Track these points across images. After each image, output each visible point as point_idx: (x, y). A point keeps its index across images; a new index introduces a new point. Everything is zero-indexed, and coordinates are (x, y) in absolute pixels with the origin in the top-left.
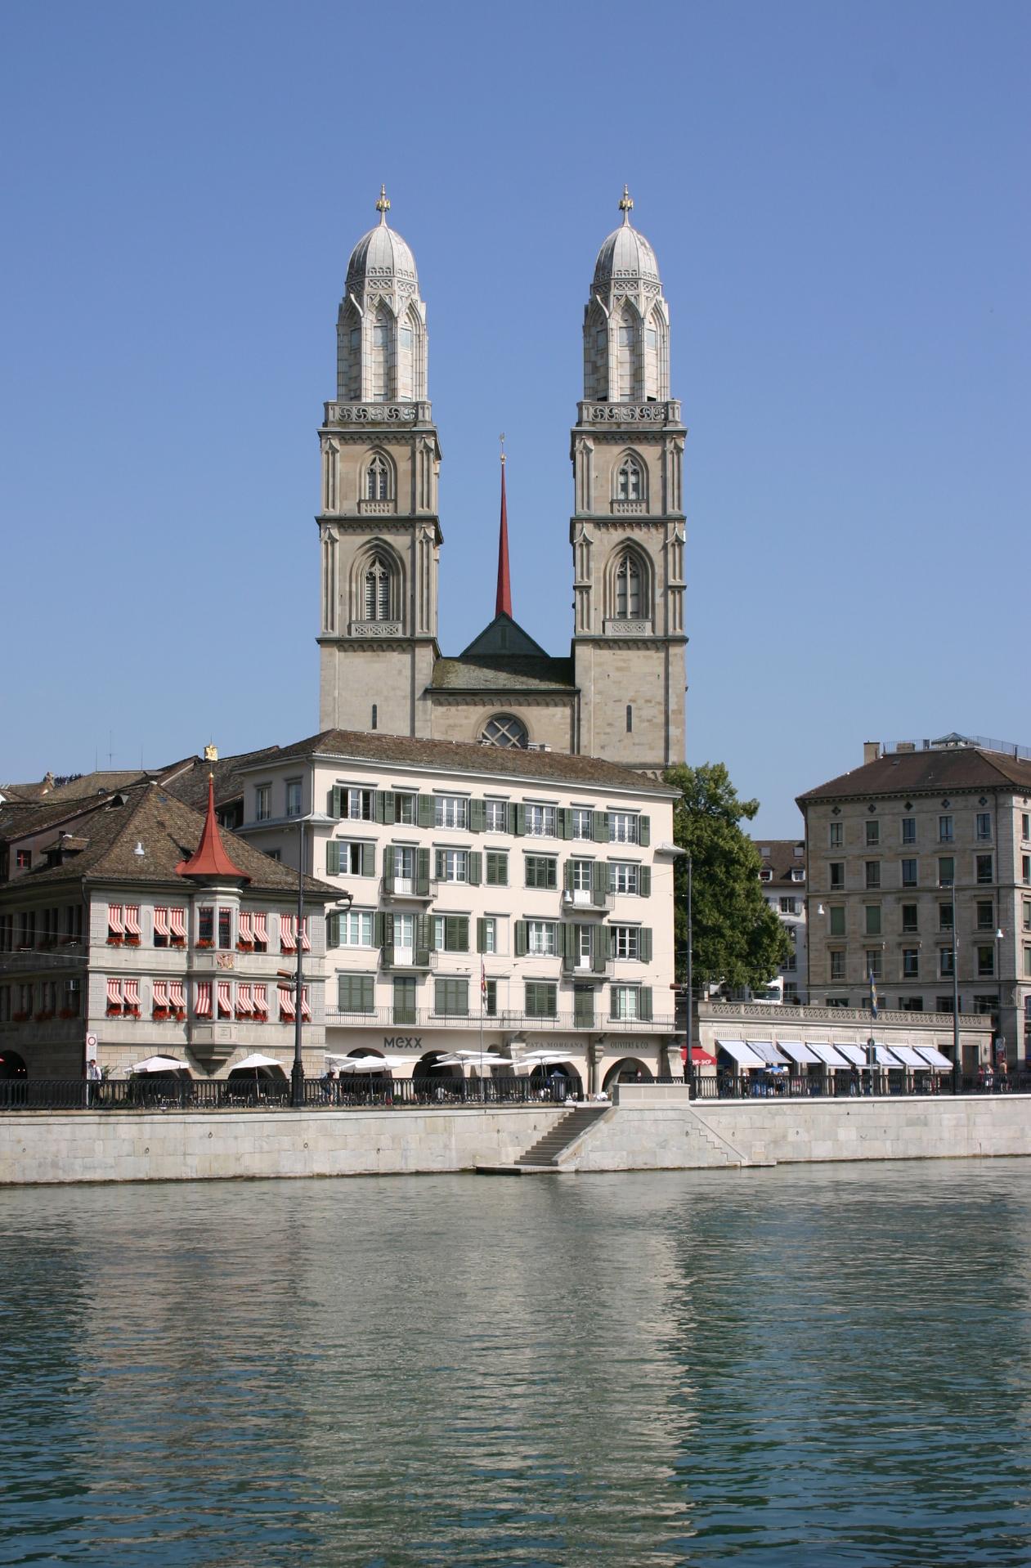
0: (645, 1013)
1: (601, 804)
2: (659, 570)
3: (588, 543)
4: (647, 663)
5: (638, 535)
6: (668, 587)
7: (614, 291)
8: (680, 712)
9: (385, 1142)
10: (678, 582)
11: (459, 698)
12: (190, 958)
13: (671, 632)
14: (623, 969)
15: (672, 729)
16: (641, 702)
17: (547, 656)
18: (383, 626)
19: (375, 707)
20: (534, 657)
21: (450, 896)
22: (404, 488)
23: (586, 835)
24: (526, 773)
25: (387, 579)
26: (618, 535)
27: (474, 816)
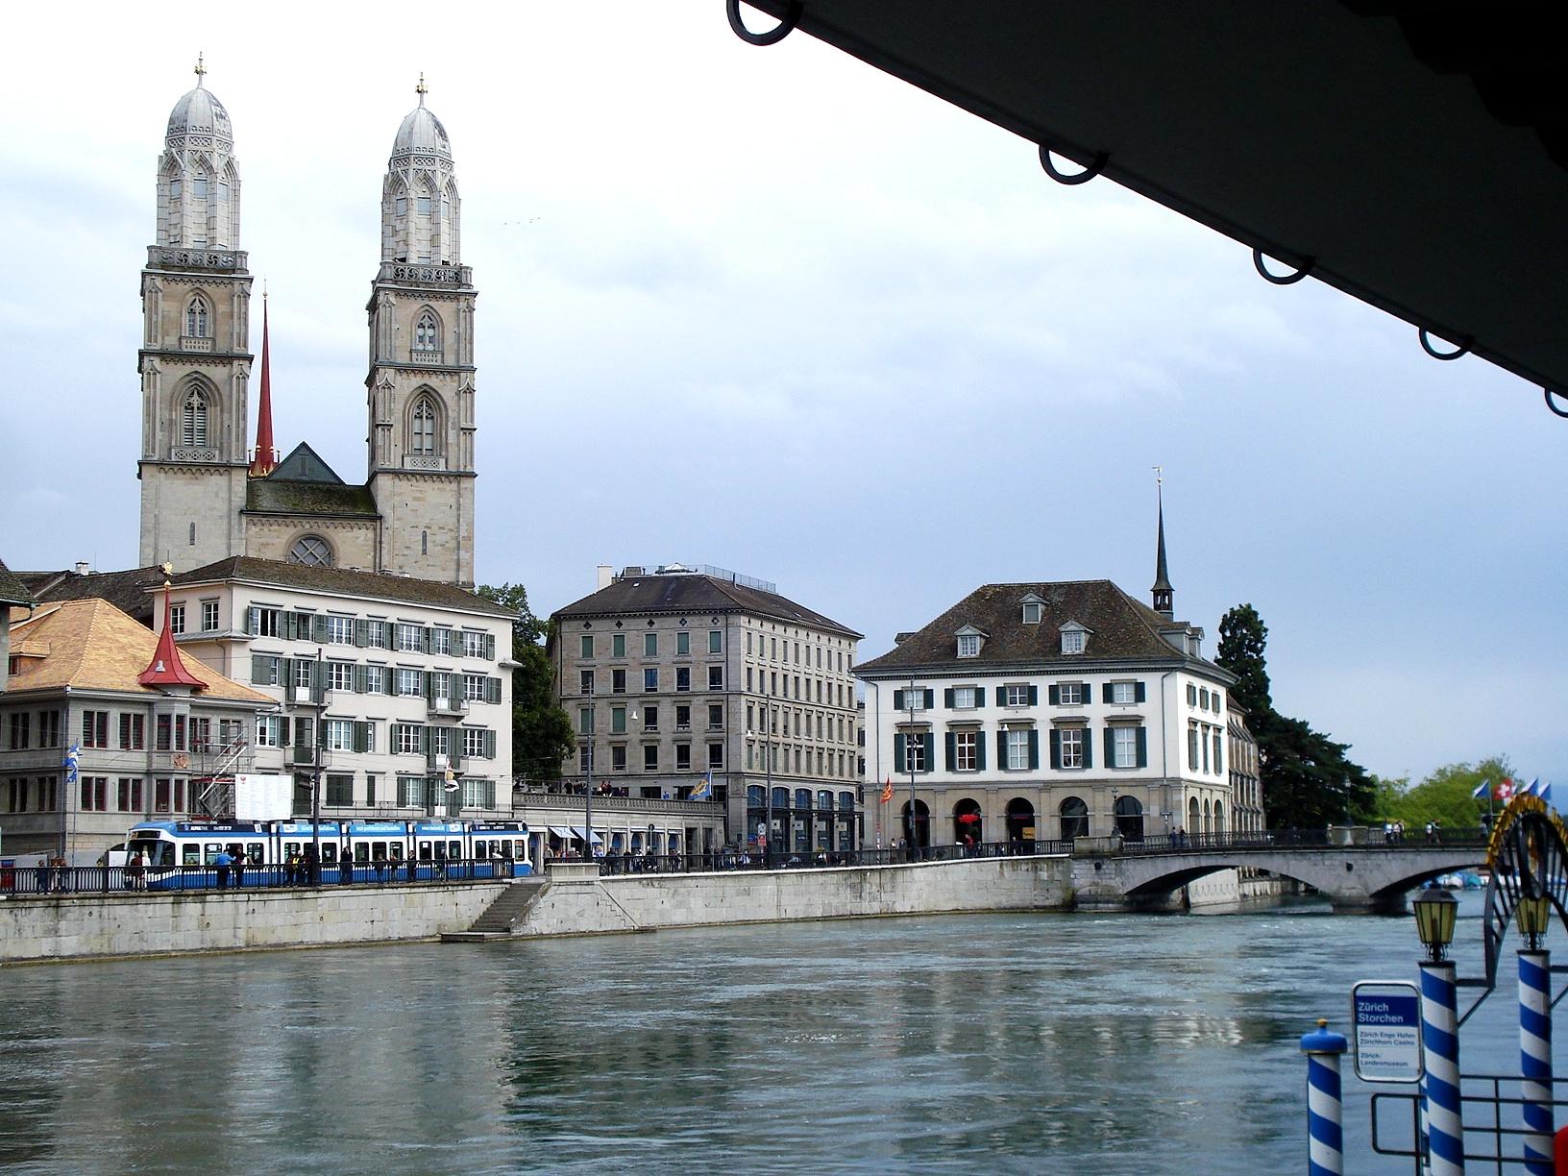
0: (490, 804)
1: (458, 623)
3: (388, 386)
5: (434, 381)
8: (470, 538)
9: (377, 915)
12: (149, 758)
14: (474, 766)
16: (435, 528)
18: (201, 451)
19: (193, 526)
22: (223, 328)
23: (446, 651)
24: (407, 599)
26: (416, 381)
27: (358, 633)
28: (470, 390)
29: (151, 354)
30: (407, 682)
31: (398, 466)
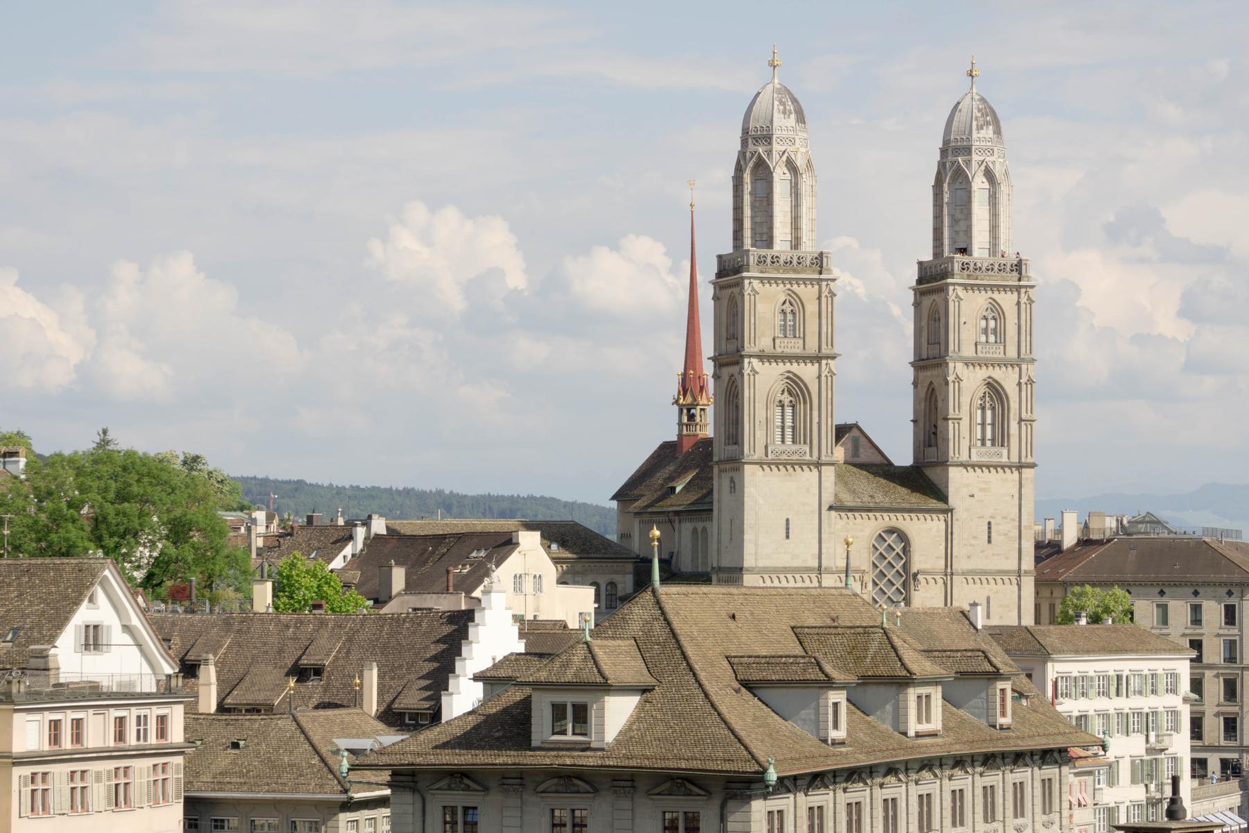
2: (1014, 405)
5: (997, 374)
6: (1021, 420)
7: (976, 157)
13: (1023, 460)
15: (1023, 541)
17: (890, 464)
19: (787, 520)
22: (812, 327)
26: (982, 374)
29: (750, 356)
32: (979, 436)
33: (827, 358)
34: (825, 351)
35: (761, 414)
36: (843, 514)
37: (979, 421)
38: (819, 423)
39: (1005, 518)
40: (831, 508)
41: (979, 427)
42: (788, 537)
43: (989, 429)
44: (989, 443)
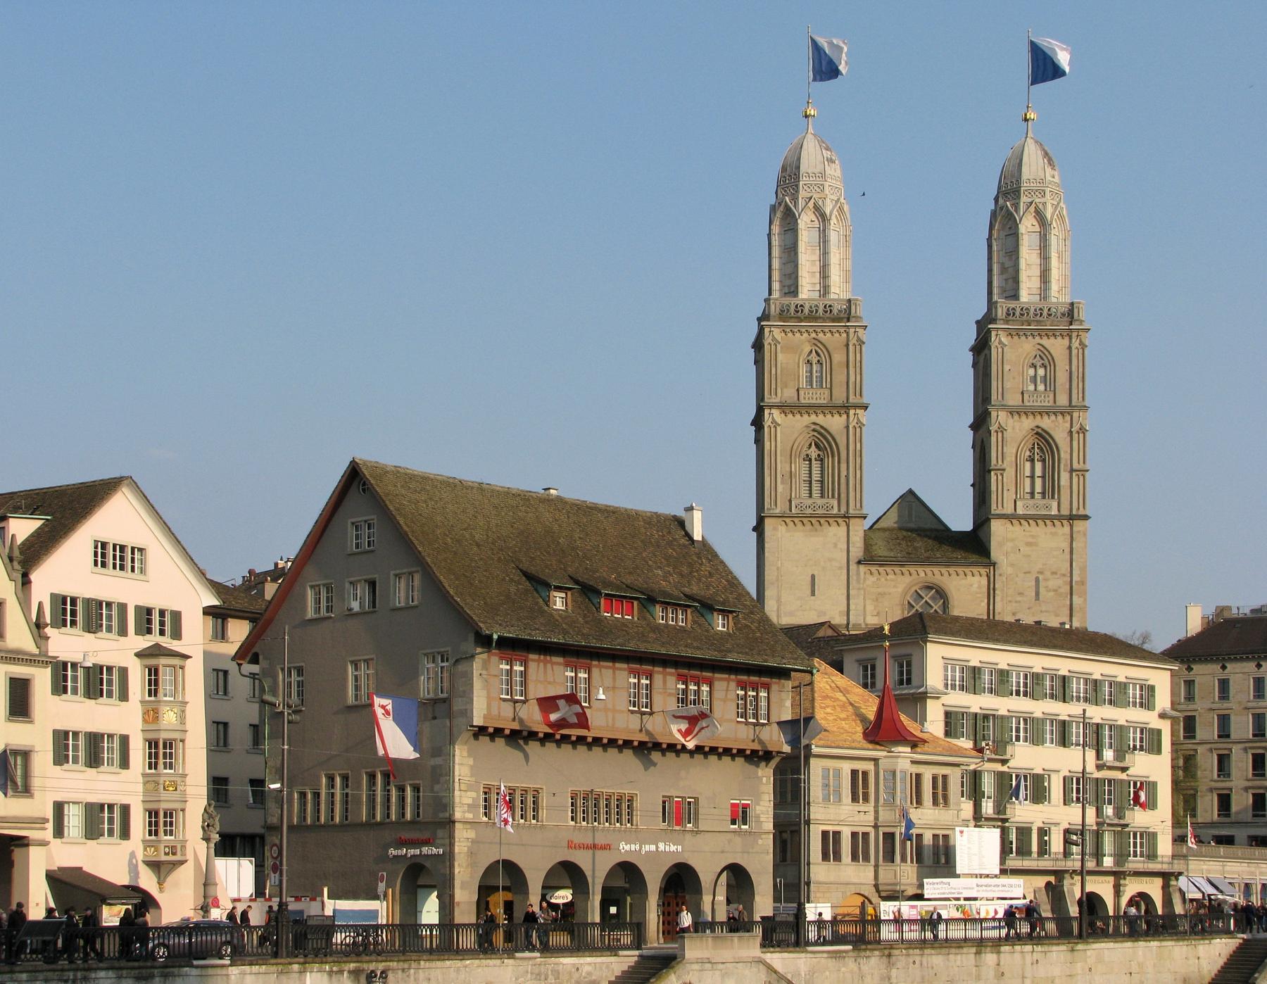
0: (1152, 856)
2: (1064, 455)
3: (1002, 429)
4: (1052, 539)
5: (1046, 423)
6: (1072, 471)
8: (1083, 583)
10: (1081, 466)
11: (889, 569)
14: (1139, 818)
15: (1075, 598)
16: (1048, 574)
18: (820, 502)
19: (813, 577)
20: (937, 530)
21: (1024, 757)
22: (840, 377)
23: (1110, 702)
25: (822, 460)
26: (1028, 423)
28: (1082, 430)
29: (771, 407)
30: (1076, 732)
31: (1009, 509)
32: (1028, 489)
33: (856, 407)
34: (852, 399)
35: (783, 467)
36: (873, 569)
37: (1028, 473)
38: (847, 477)
39: (1054, 573)
40: (859, 562)
41: (1028, 481)
42: (813, 593)
43: (1038, 482)
44: (1037, 496)
